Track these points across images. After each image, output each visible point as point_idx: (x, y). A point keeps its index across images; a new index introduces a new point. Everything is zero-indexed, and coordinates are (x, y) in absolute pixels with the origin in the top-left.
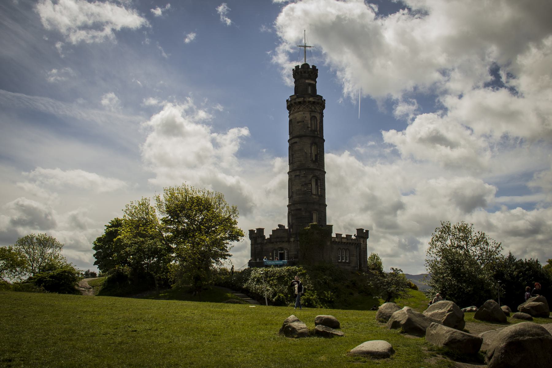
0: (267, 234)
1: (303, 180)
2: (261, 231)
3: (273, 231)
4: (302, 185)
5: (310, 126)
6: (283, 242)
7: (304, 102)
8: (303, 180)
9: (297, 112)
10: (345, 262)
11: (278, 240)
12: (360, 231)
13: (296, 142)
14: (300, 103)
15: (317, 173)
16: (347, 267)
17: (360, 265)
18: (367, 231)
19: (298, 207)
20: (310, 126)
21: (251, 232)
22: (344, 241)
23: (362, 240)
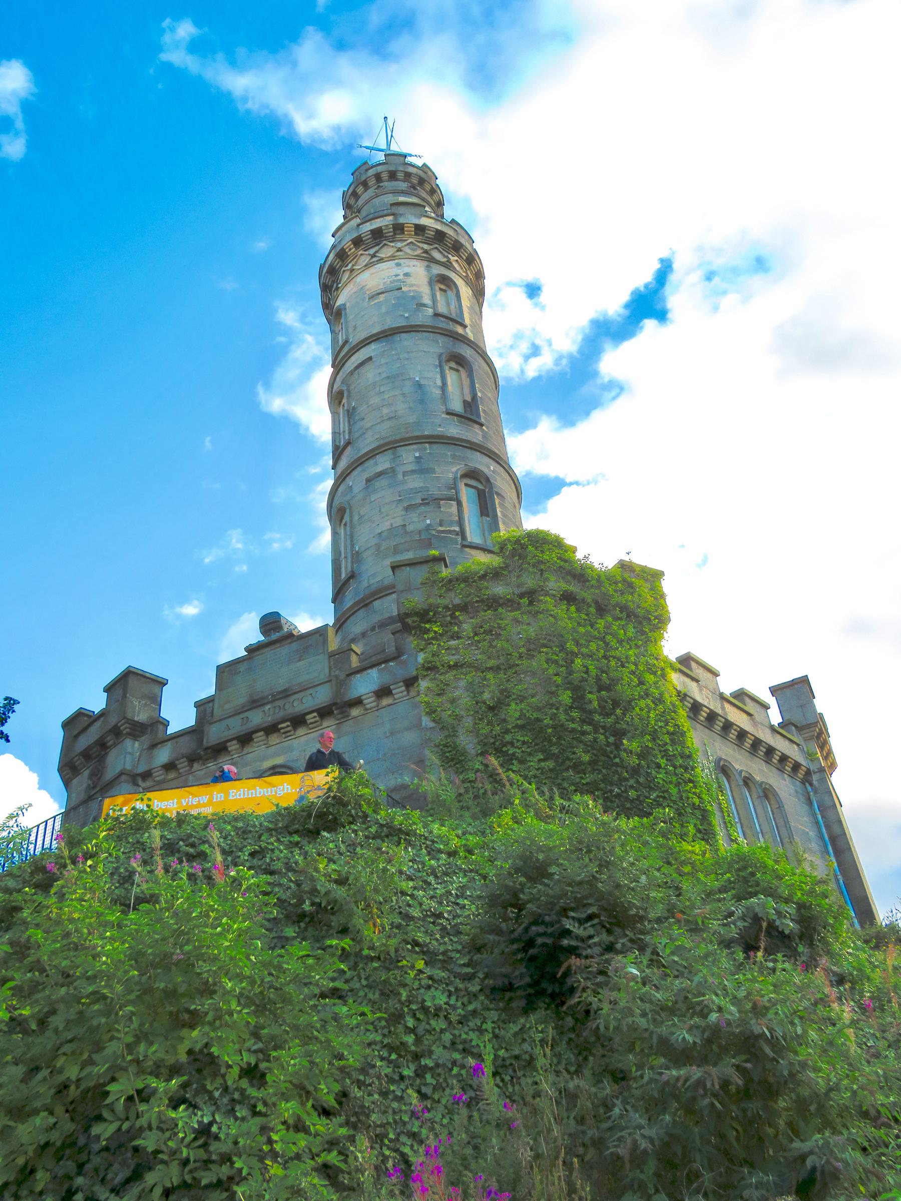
1: (415, 482)
4: (407, 509)
5: (427, 300)
6: (298, 721)
7: (399, 228)
8: (415, 482)
9: (368, 266)
11: (257, 718)
13: (370, 359)
14: (378, 234)
20: (427, 300)
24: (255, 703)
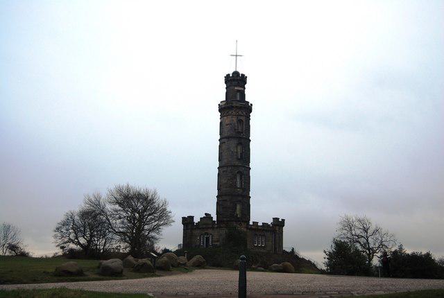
0: (196, 220)
2: (191, 218)
3: (201, 218)
10: (261, 247)
11: (204, 226)
12: (276, 220)
15: (242, 169)
16: (262, 251)
17: (275, 248)
18: (283, 220)
19: (225, 198)
21: (184, 218)
22: (260, 228)
23: (277, 228)
24: (204, 224)
